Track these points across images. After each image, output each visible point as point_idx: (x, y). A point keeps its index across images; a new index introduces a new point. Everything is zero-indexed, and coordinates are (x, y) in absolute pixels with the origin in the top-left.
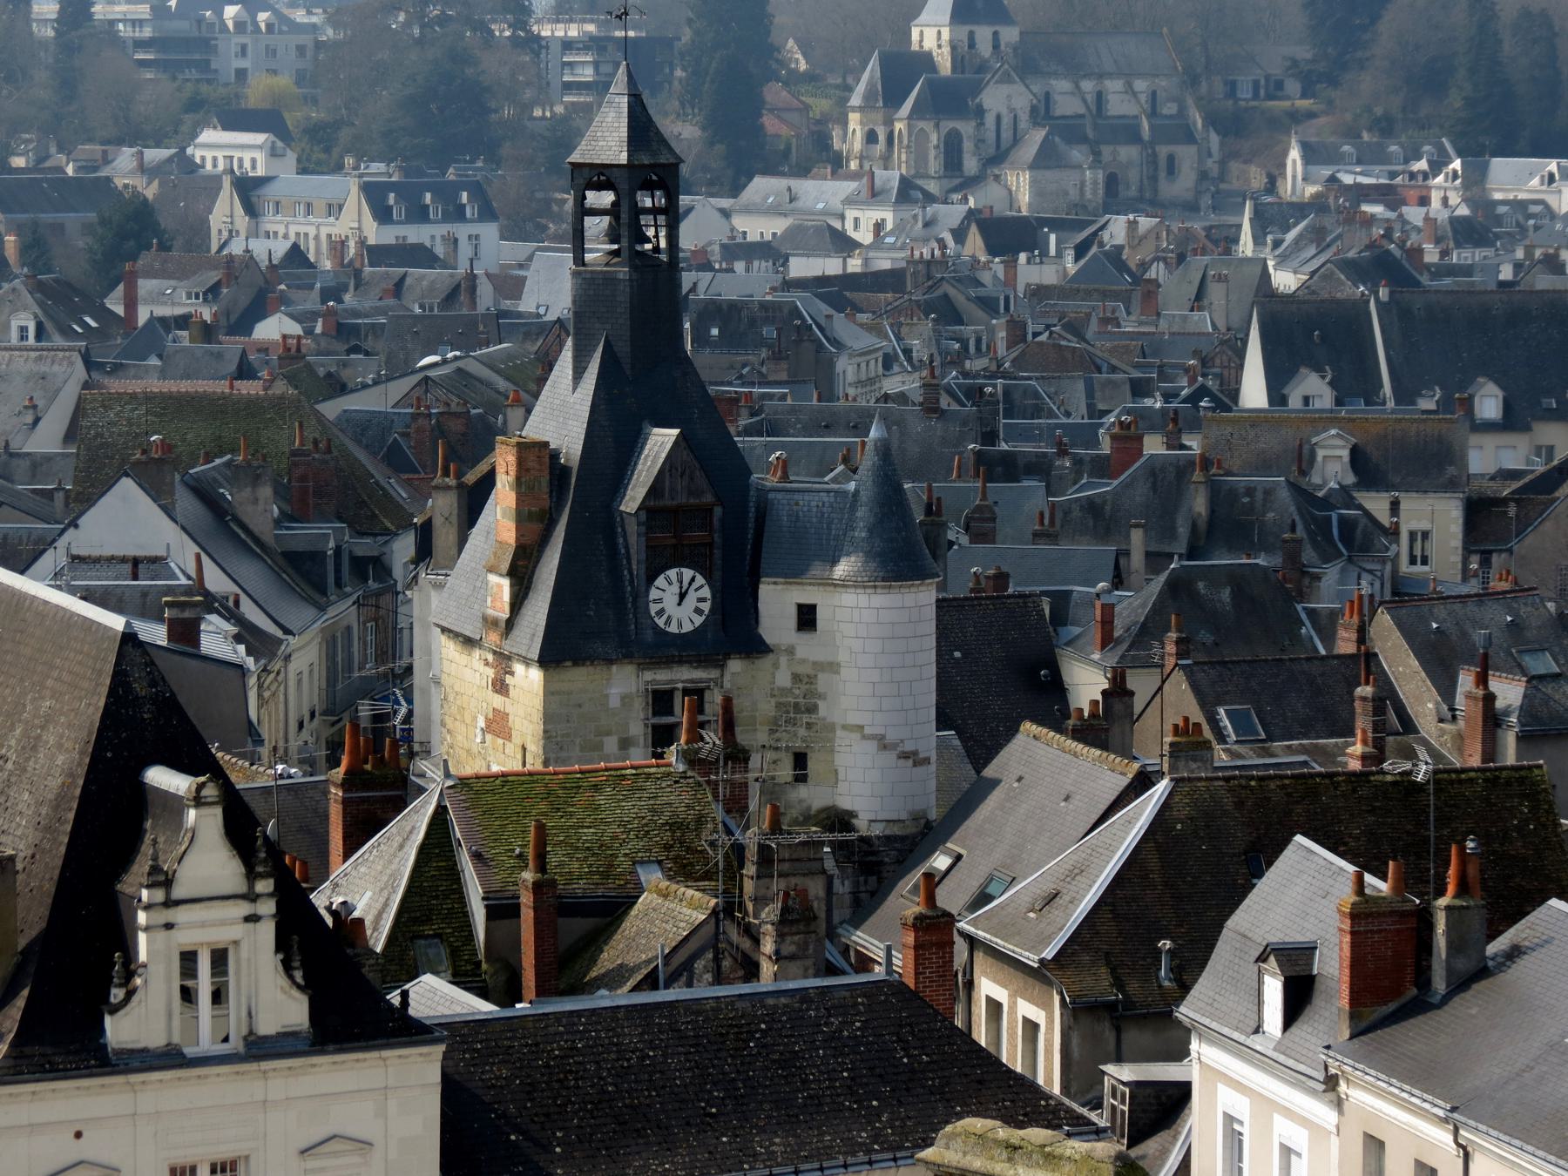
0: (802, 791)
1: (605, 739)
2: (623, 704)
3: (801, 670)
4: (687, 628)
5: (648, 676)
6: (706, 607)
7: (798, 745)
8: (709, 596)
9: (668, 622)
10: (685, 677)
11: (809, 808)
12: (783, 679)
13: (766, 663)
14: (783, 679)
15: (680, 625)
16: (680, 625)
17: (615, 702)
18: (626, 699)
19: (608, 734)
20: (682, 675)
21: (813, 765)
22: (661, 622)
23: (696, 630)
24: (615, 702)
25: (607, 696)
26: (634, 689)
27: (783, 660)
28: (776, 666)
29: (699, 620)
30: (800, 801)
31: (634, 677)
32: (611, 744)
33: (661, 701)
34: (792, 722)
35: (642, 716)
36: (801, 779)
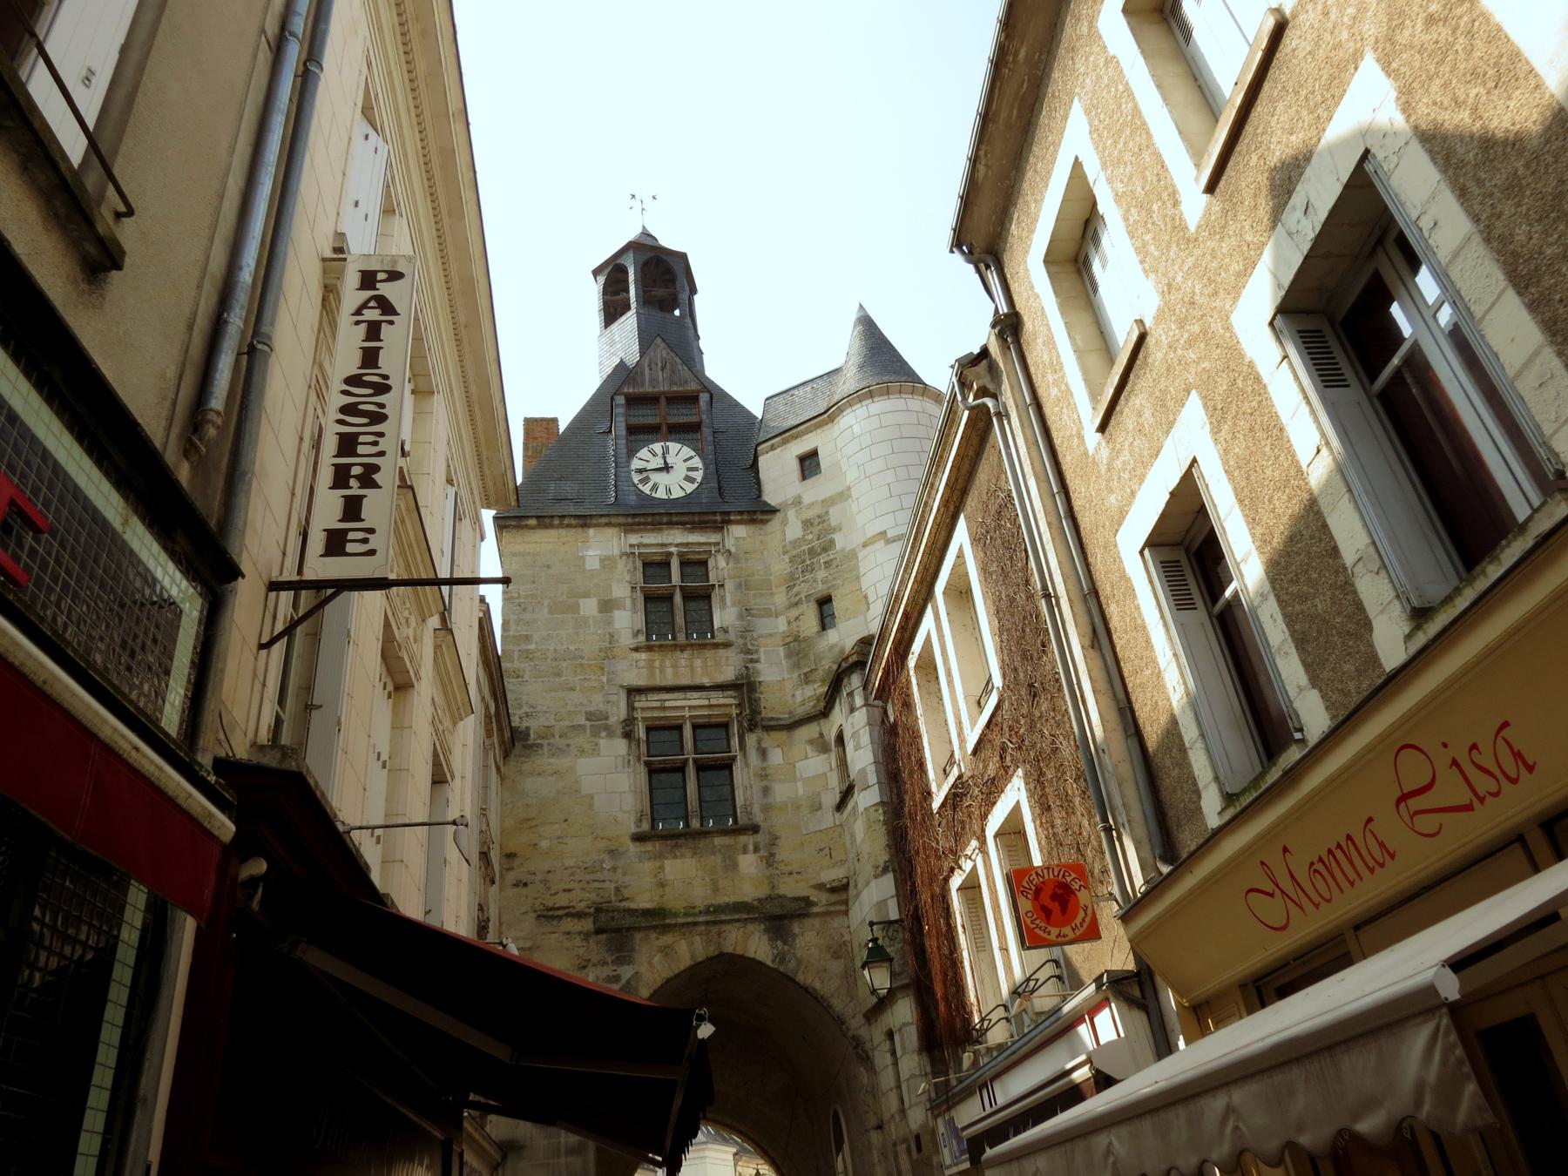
0: (832, 636)
1: (581, 601)
2: (603, 566)
3: (808, 514)
4: (677, 493)
5: (634, 539)
6: (698, 476)
7: (820, 589)
8: (700, 465)
9: (655, 488)
10: (679, 541)
11: (843, 650)
12: (794, 530)
13: (776, 521)
14: (794, 530)
15: (669, 491)
16: (669, 491)
17: (592, 563)
18: (606, 562)
19: (586, 595)
20: (675, 538)
21: (838, 605)
22: (646, 489)
23: (688, 496)
24: (592, 563)
25: (583, 557)
26: (616, 552)
27: (791, 514)
28: (785, 523)
29: (690, 488)
30: (831, 648)
31: (615, 540)
32: (589, 607)
33: (654, 566)
34: (811, 569)
35: (628, 578)
36: (826, 619)
